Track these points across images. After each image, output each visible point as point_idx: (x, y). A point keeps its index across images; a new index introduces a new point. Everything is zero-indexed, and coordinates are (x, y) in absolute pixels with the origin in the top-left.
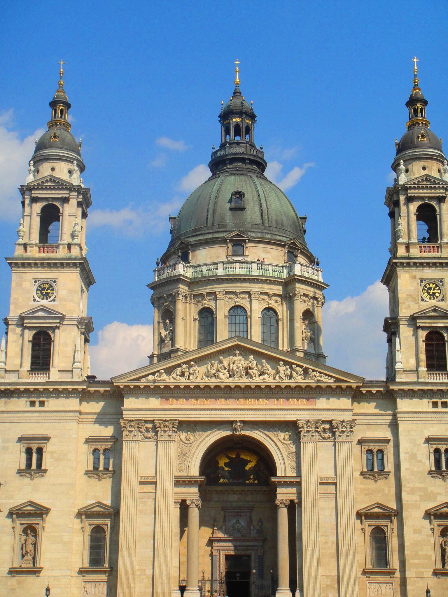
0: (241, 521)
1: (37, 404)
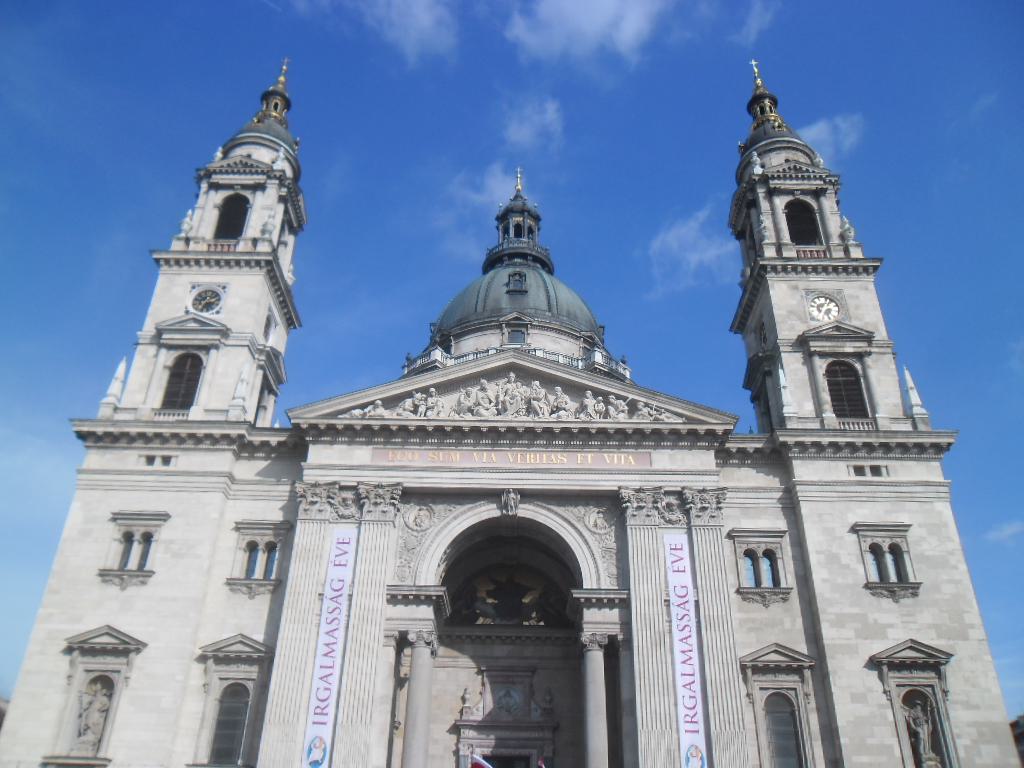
0: (512, 693)
1: (158, 461)
